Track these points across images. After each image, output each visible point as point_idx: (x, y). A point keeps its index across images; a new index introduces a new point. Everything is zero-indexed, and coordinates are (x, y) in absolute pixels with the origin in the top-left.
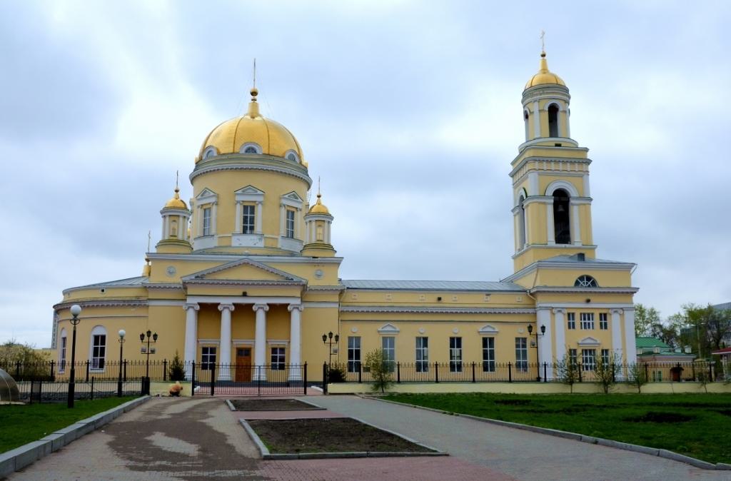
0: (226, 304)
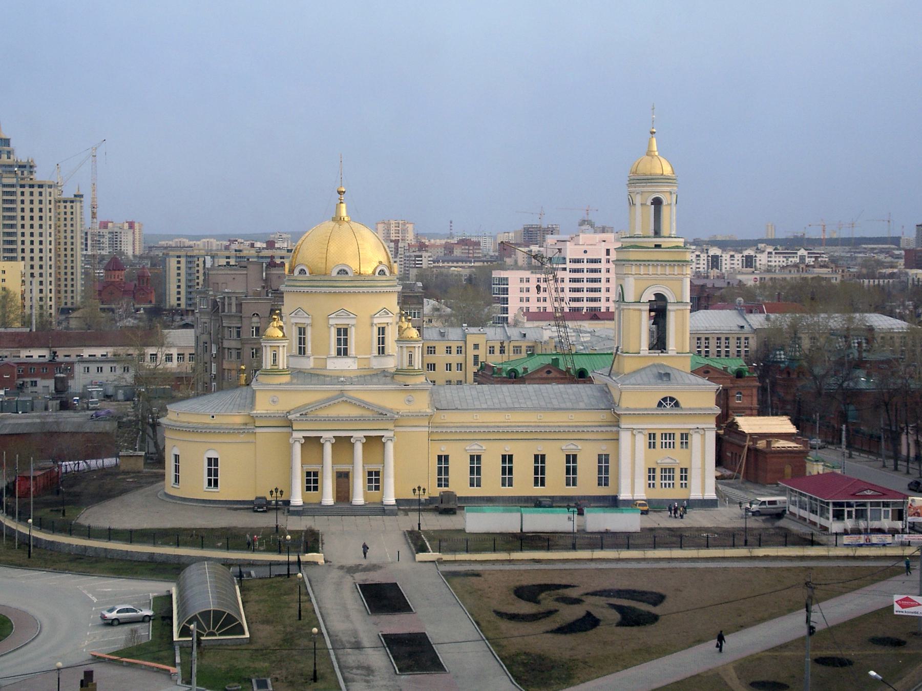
0: (328, 436)
